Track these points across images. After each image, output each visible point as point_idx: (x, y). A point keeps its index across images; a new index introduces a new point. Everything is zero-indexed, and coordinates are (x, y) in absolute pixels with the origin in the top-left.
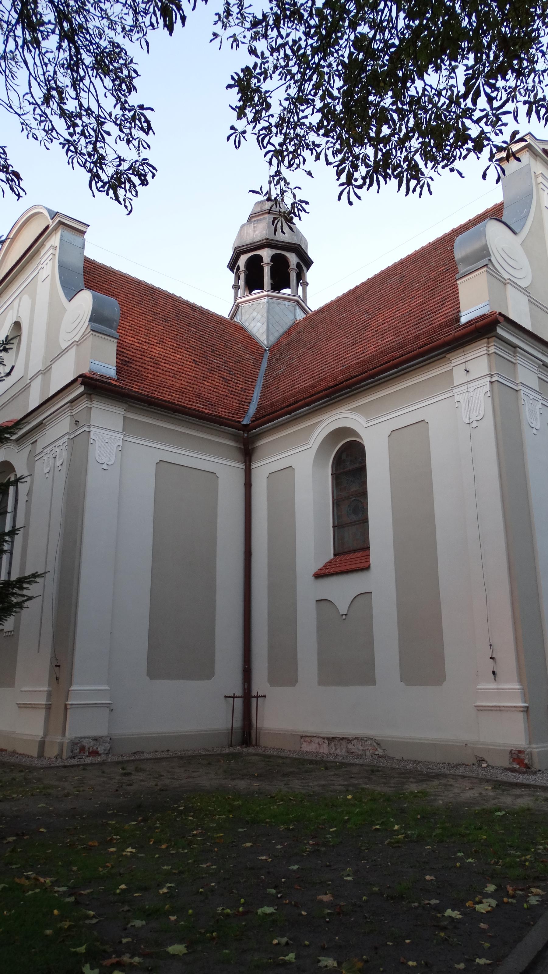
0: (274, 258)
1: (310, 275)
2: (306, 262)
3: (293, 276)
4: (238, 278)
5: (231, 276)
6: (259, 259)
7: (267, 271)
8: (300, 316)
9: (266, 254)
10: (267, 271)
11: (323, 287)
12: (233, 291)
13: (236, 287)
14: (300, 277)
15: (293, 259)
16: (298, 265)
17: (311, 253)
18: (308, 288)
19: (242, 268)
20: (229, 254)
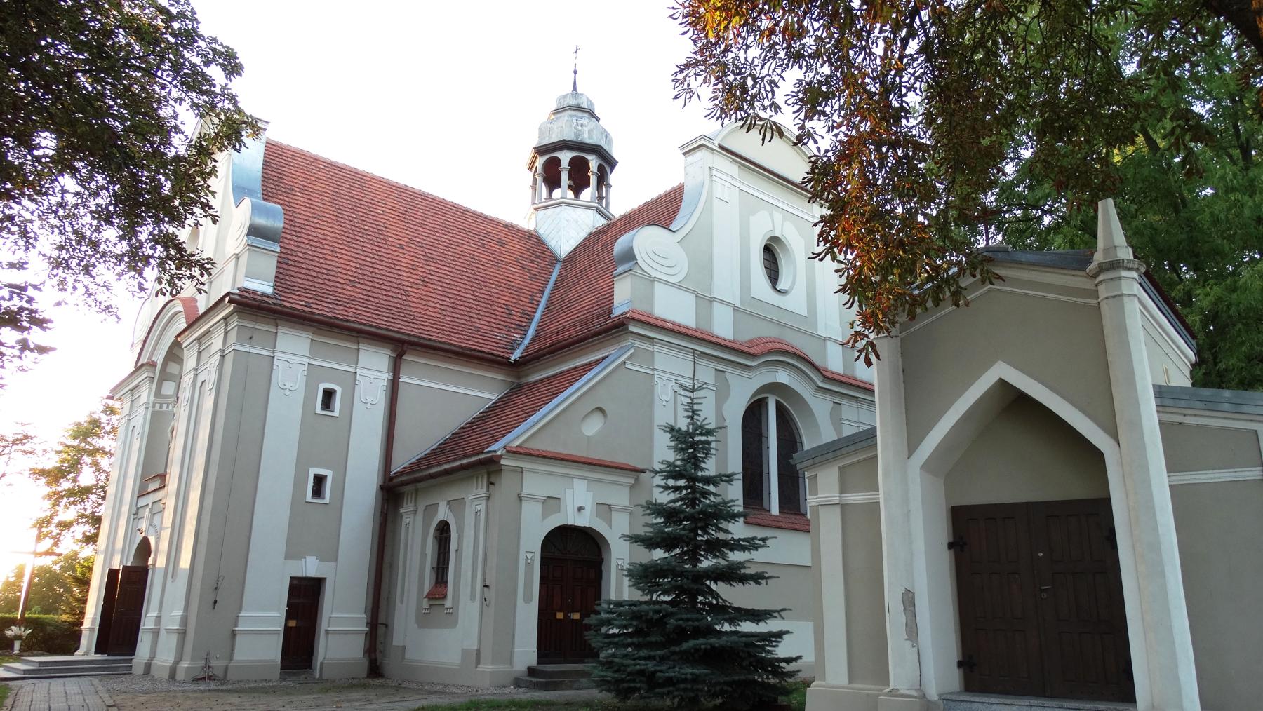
0: (573, 162)
1: (614, 178)
2: (608, 162)
3: (593, 180)
4: (535, 180)
5: (529, 175)
6: (557, 162)
7: (564, 177)
8: (602, 222)
9: (565, 157)
10: (564, 177)
11: (626, 193)
12: (530, 191)
13: (534, 187)
14: (602, 179)
15: (594, 162)
16: (601, 168)
17: (615, 153)
18: (611, 190)
19: (539, 170)
20: (529, 154)
